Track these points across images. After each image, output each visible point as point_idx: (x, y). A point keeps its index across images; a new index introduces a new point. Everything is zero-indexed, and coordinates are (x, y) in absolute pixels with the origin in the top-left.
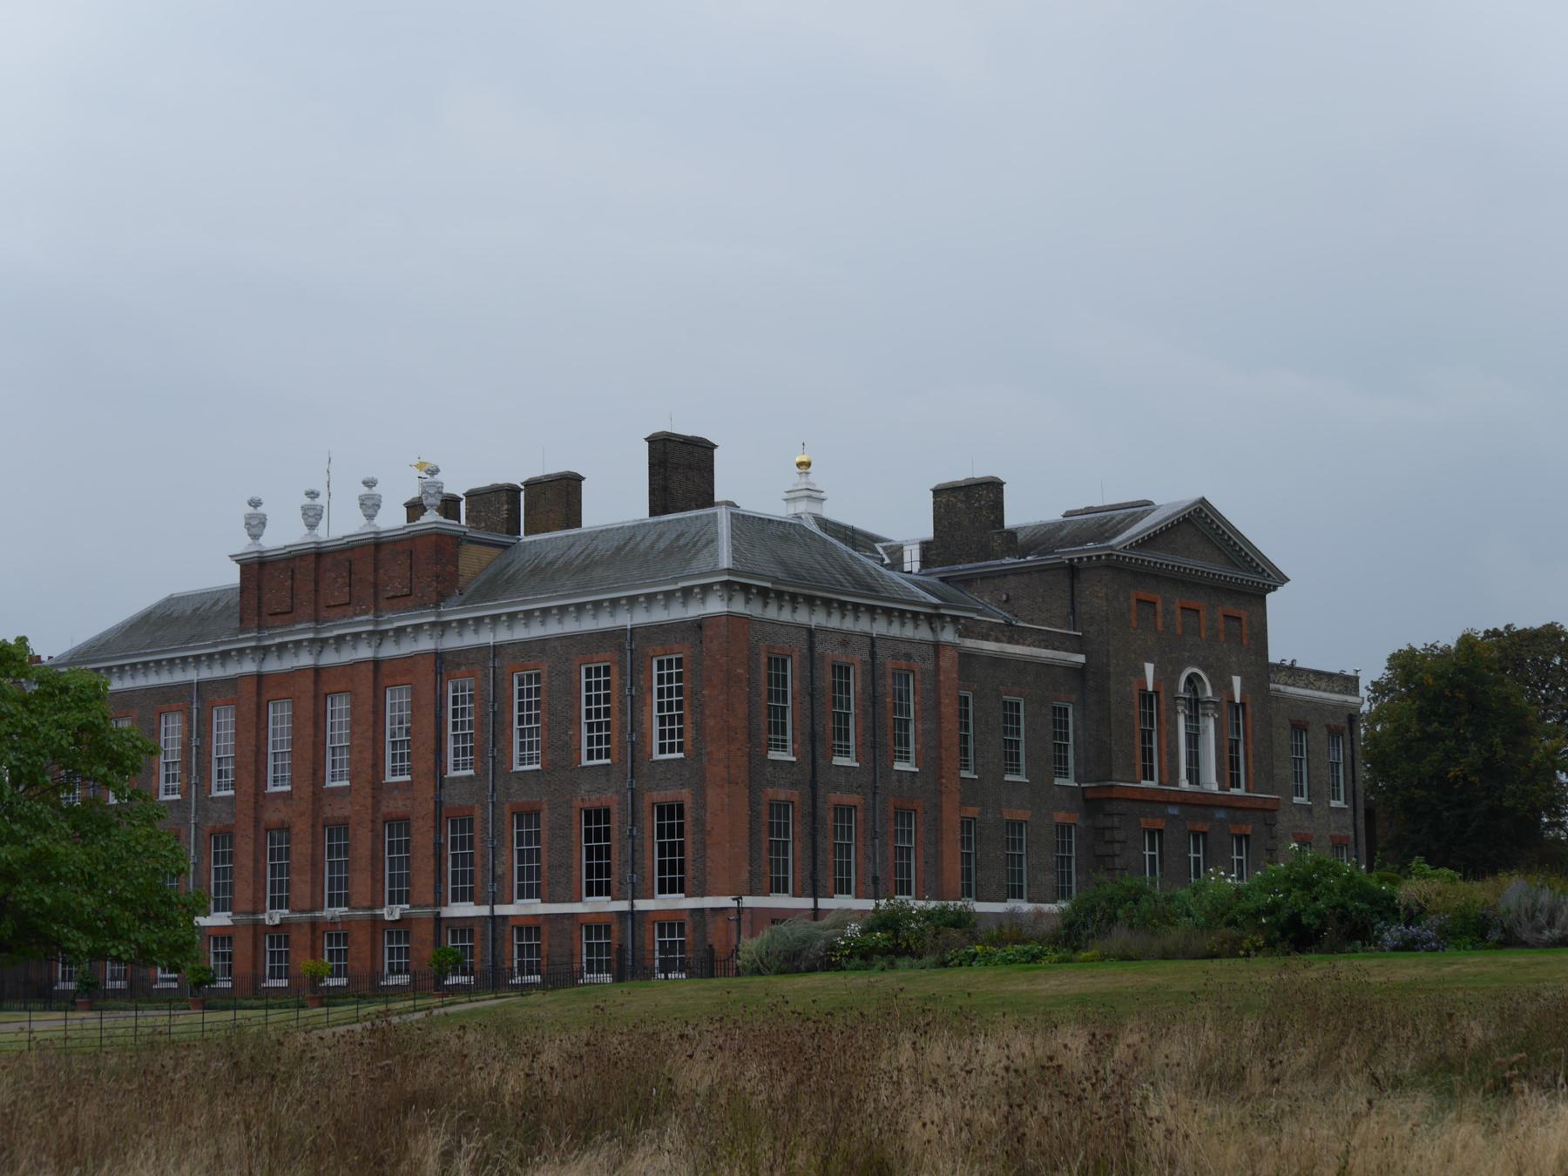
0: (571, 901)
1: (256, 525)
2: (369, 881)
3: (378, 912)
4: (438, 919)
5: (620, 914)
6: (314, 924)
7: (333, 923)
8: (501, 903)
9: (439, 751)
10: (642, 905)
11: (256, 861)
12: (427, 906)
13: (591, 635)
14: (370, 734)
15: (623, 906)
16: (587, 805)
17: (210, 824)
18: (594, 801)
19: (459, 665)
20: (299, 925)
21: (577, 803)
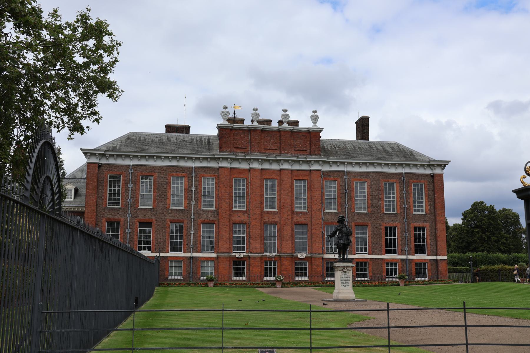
0: (381, 255)
1: (224, 115)
2: (291, 244)
3: (295, 255)
4: (323, 258)
5: (402, 260)
6: (261, 258)
7: (270, 258)
8: (351, 254)
9: (322, 203)
10: (410, 257)
11: (229, 234)
12: (320, 254)
13: (388, 173)
14: (290, 194)
15: (404, 257)
16: (387, 225)
17: (202, 219)
18: (390, 224)
19: (330, 176)
20: (254, 258)
21: (384, 225)
